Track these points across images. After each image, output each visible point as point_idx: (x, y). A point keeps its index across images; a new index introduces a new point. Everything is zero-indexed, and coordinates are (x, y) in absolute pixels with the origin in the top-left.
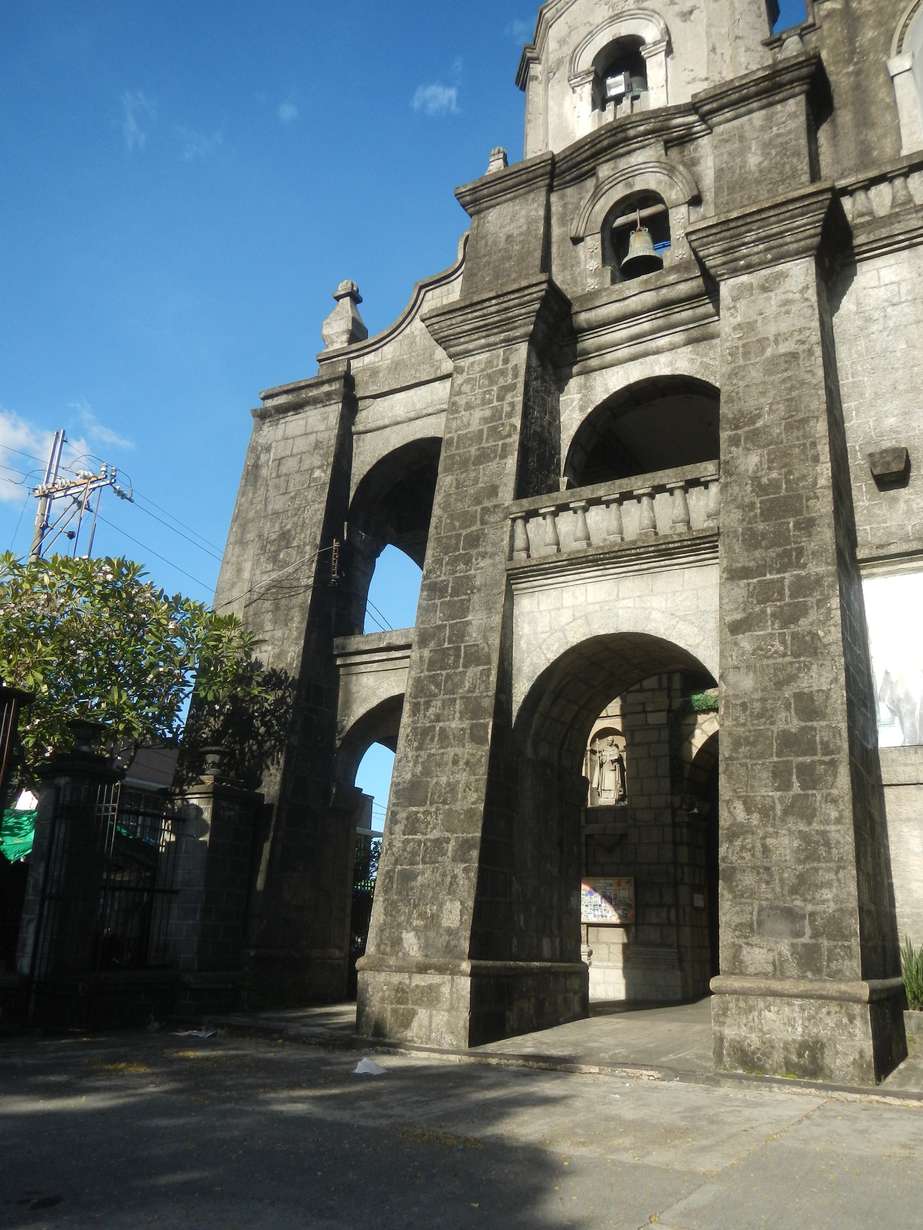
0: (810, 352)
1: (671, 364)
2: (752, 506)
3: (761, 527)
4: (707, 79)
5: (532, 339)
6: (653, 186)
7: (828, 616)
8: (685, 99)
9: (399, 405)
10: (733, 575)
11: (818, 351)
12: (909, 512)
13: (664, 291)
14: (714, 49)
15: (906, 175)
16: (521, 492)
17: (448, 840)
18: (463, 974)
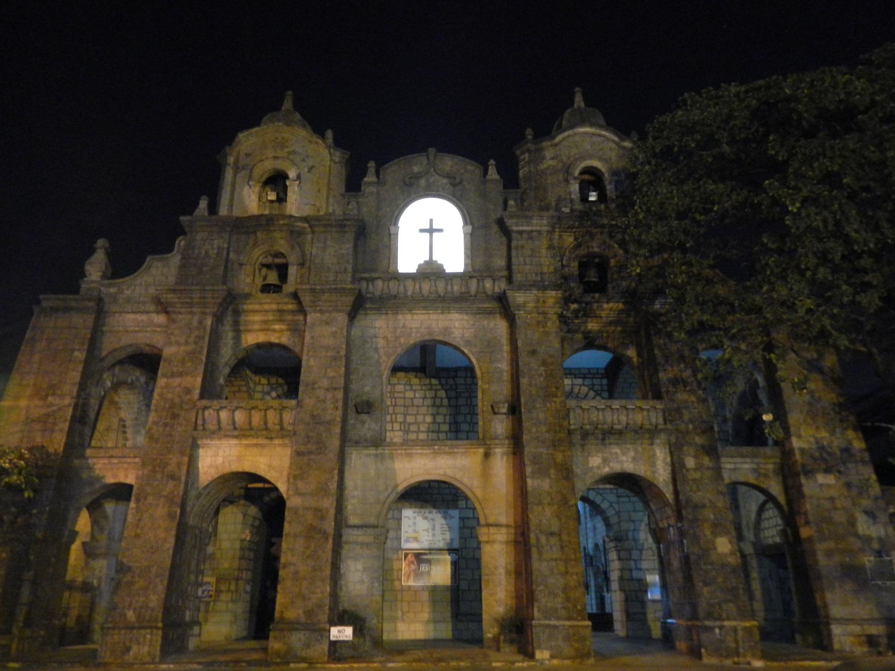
0: (341, 357)
1: (279, 338)
2: (309, 424)
3: (311, 434)
4: (314, 205)
5: (214, 315)
6: (283, 251)
7: (333, 477)
8: (305, 214)
9: (130, 319)
10: (299, 454)
11: (344, 360)
12: (369, 429)
13: (281, 306)
14: (319, 191)
15: (389, 280)
16: (202, 396)
17: (153, 566)
18: (157, 628)
